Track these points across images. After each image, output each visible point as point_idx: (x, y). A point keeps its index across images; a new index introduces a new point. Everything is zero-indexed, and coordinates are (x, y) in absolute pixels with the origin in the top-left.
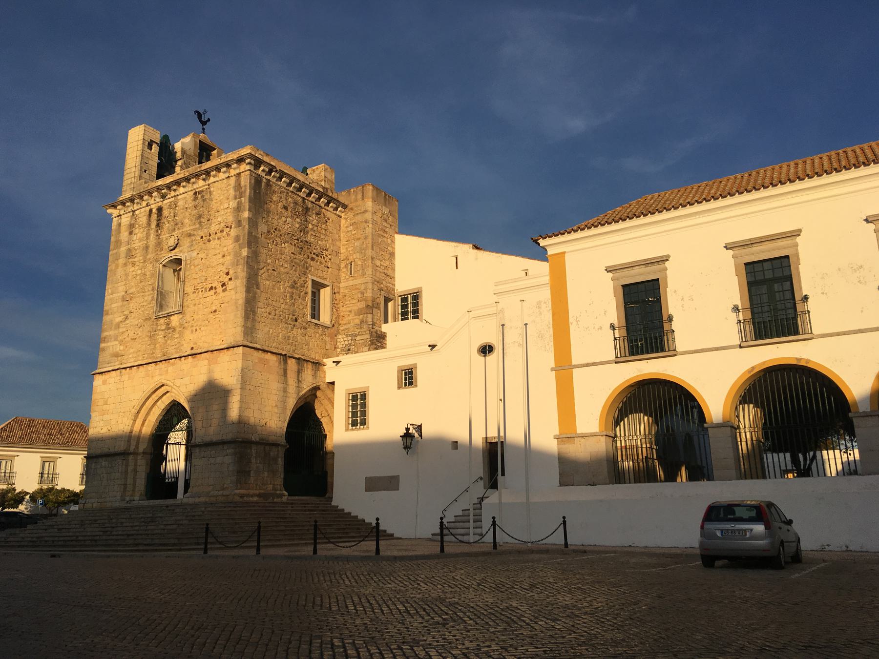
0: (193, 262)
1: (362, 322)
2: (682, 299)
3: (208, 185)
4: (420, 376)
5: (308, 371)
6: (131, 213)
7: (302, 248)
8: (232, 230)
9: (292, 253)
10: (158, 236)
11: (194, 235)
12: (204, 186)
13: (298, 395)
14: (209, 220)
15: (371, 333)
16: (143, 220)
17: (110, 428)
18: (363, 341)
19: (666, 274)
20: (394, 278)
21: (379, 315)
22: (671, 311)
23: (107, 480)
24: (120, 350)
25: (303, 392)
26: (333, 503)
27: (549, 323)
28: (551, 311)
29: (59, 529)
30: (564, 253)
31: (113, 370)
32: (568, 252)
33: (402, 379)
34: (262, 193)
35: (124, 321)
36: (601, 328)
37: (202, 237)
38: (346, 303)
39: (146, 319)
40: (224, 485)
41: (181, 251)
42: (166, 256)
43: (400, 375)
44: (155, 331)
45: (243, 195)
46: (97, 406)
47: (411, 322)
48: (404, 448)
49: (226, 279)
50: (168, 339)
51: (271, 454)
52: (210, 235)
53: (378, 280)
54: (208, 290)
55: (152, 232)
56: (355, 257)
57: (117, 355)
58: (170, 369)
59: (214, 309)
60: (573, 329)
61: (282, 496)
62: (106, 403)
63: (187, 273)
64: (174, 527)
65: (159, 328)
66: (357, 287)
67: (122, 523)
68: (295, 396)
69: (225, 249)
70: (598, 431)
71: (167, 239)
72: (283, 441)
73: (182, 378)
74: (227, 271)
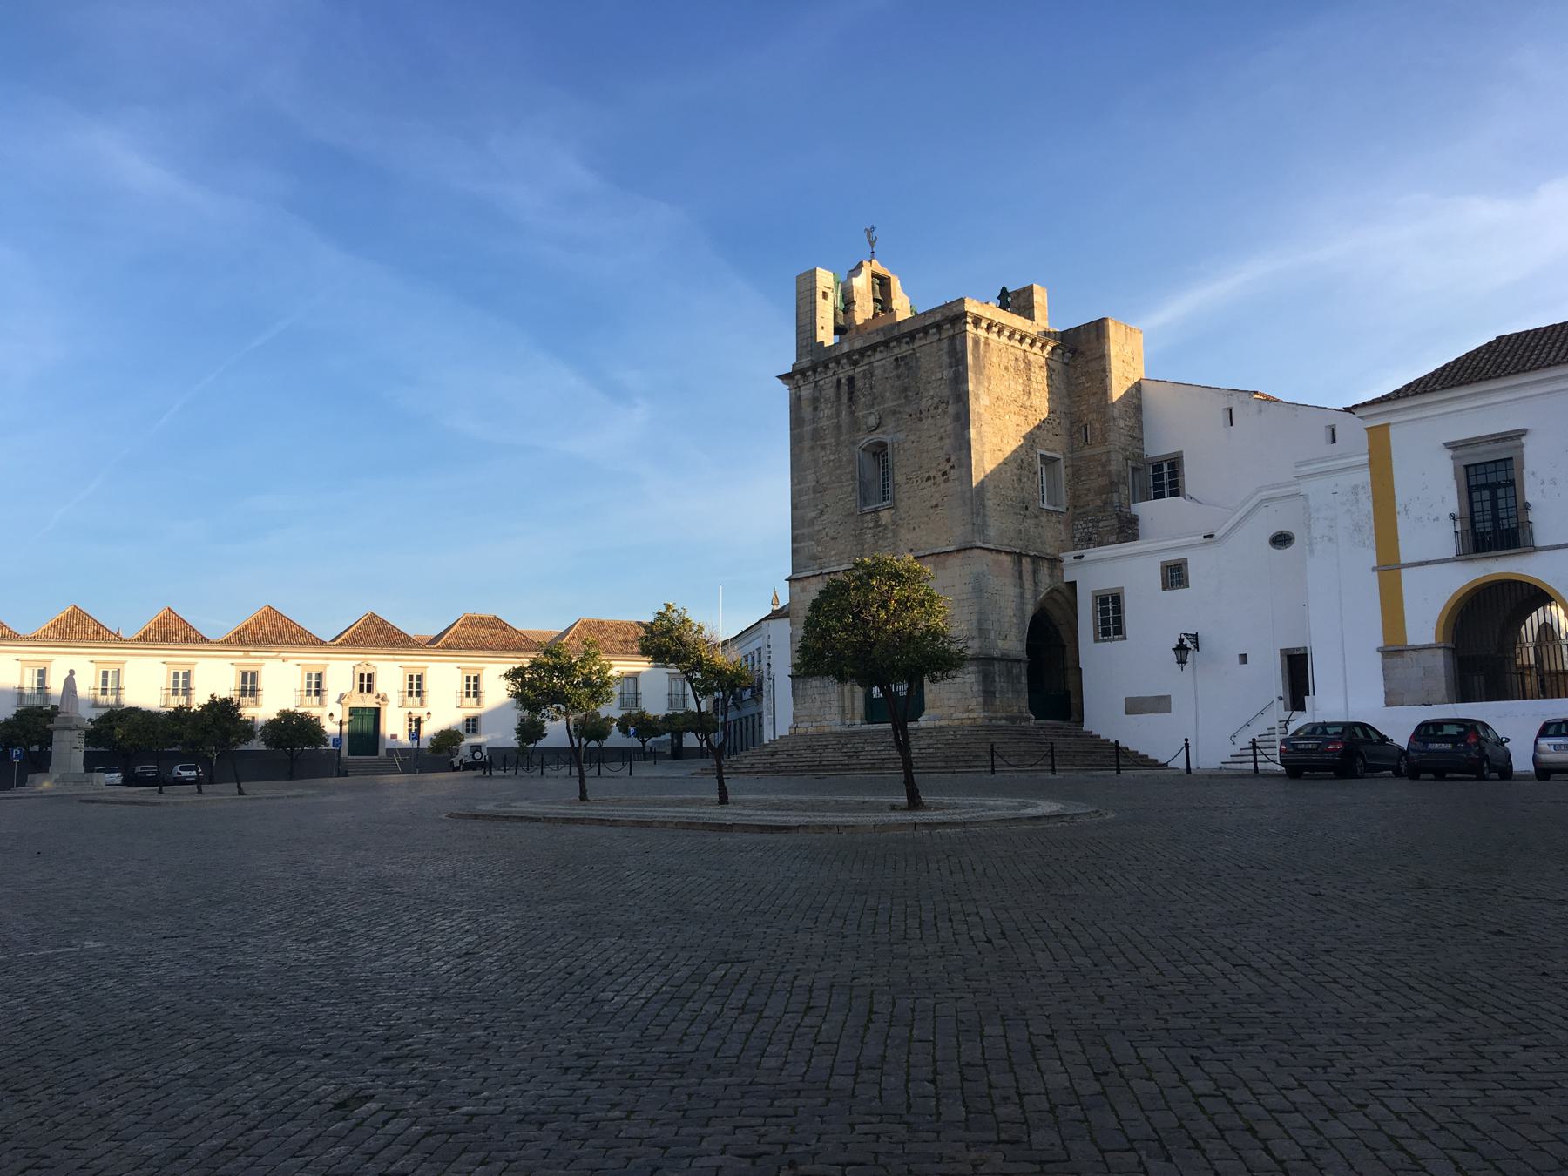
0: (901, 446)
1: (1105, 503)
2: (1543, 483)
3: (913, 349)
4: (1193, 573)
5: (1045, 570)
6: (813, 384)
7: (1026, 416)
8: (949, 407)
9: (1018, 425)
10: (852, 413)
11: (900, 412)
12: (907, 351)
13: (1036, 599)
14: (917, 394)
15: (1119, 518)
16: (830, 392)
18: (1108, 528)
19: (1522, 451)
20: (1142, 439)
21: (1127, 492)
22: (1528, 499)
23: (821, 702)
24: (818, 551)
25: (1041, 596)
26: (1085, 728)
27: (1369, 512)
28: (1371, 498)
29: (788, 755)
30: (1389, 424)
31: (813, 576)
32: (1394, 424)
33: (1167, 576)
34: (981, 356)
35: (819, 517)
36: (1437, 519)
37: (910, 416)
38: (1083, 479)
39: (846, 516)
41: (884, 433)
42: (866, 440)
43: (1165, 573)
44: (861, 529)
45: (961, 362)
46: (798, 617)
47: (1168, 502)
48: (1178, 663)
50: (879, 539)
51: (1014, 671)
52: (921, 413)
53: (1123, 446)
55: (844, 407)
56: (1090, 418)
57: (814, 558)
59: (934, 503)
60: (1401, 522)
61: (1028, 719)
63: (896, 460)
64: (931, 750)
65: (866, 525)
66: (1096, 457)
67: (863, 748)
68: (1032, 601)
69: (943, 429)
70: (1433, 641)
71: (863, 417)
72: (1024, 656)
74: (948, 456)
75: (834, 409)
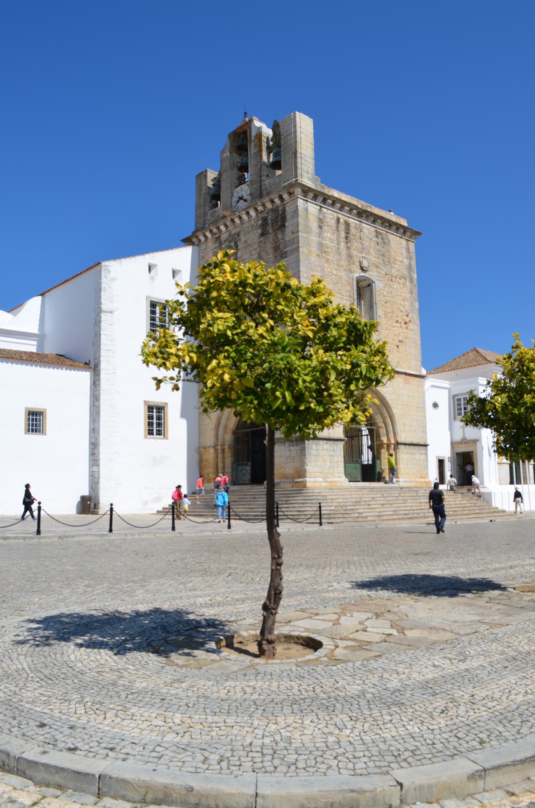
10: (348, 248)
23: (331, 462)
49: (407, 320)
75: (335, 236)
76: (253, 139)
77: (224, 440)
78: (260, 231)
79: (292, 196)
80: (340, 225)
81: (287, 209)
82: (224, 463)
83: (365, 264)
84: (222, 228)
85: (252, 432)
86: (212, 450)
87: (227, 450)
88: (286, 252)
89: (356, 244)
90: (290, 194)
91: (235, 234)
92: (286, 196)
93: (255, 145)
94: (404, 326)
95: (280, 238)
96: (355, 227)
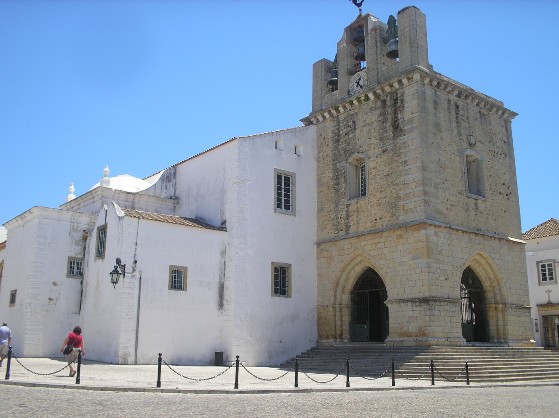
17: (446, 277)
40: (527, 336)
46: (433, 253)
49: (508, 193)
54: (499, 192)
58: (486, 242)
62: (440, 253)
73: (494, 253)
74: (508, 186)
76: (369, 31)
77: (341, 299)
78: (378, 112)
79: (411, 80)
80: (451, 107)
81: (405, 91)
82: (341, 320)
83: (472, 141)
84: (341, 109)
85: (369, 292)
86: (331, 309)
87: (344, 309)
88: (404, 130)
89: (464, 124)
90: (409, 79)
91: (353, 114)
92: (405, 81)
93: (371, 37)
94: (506, 197)
95: (399, 117)
96: (463, 110)
